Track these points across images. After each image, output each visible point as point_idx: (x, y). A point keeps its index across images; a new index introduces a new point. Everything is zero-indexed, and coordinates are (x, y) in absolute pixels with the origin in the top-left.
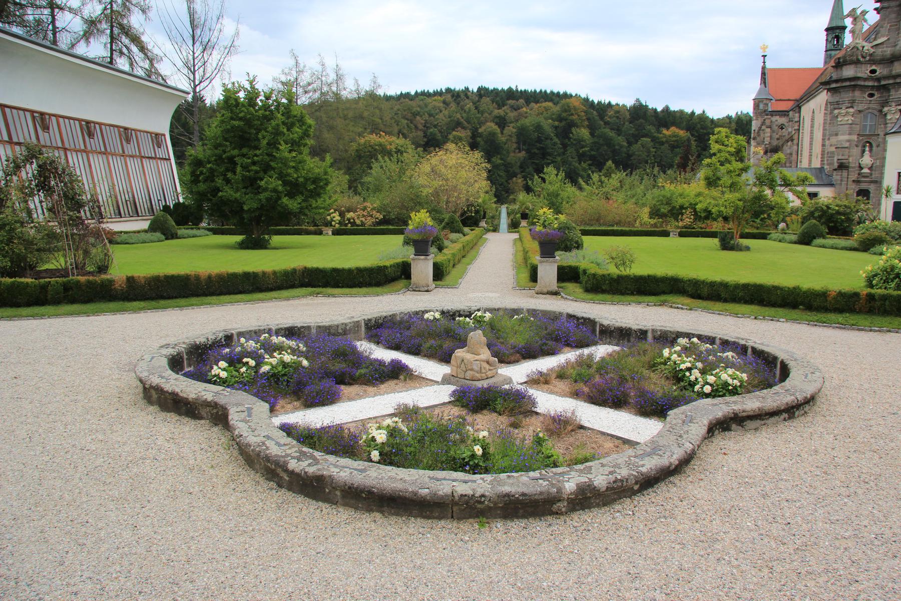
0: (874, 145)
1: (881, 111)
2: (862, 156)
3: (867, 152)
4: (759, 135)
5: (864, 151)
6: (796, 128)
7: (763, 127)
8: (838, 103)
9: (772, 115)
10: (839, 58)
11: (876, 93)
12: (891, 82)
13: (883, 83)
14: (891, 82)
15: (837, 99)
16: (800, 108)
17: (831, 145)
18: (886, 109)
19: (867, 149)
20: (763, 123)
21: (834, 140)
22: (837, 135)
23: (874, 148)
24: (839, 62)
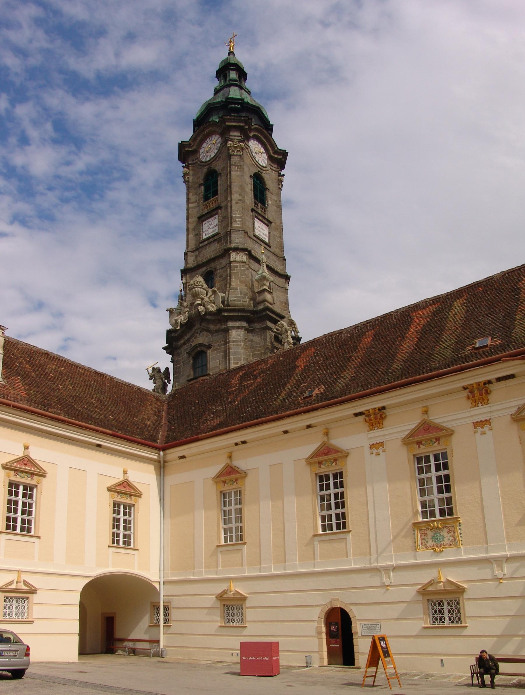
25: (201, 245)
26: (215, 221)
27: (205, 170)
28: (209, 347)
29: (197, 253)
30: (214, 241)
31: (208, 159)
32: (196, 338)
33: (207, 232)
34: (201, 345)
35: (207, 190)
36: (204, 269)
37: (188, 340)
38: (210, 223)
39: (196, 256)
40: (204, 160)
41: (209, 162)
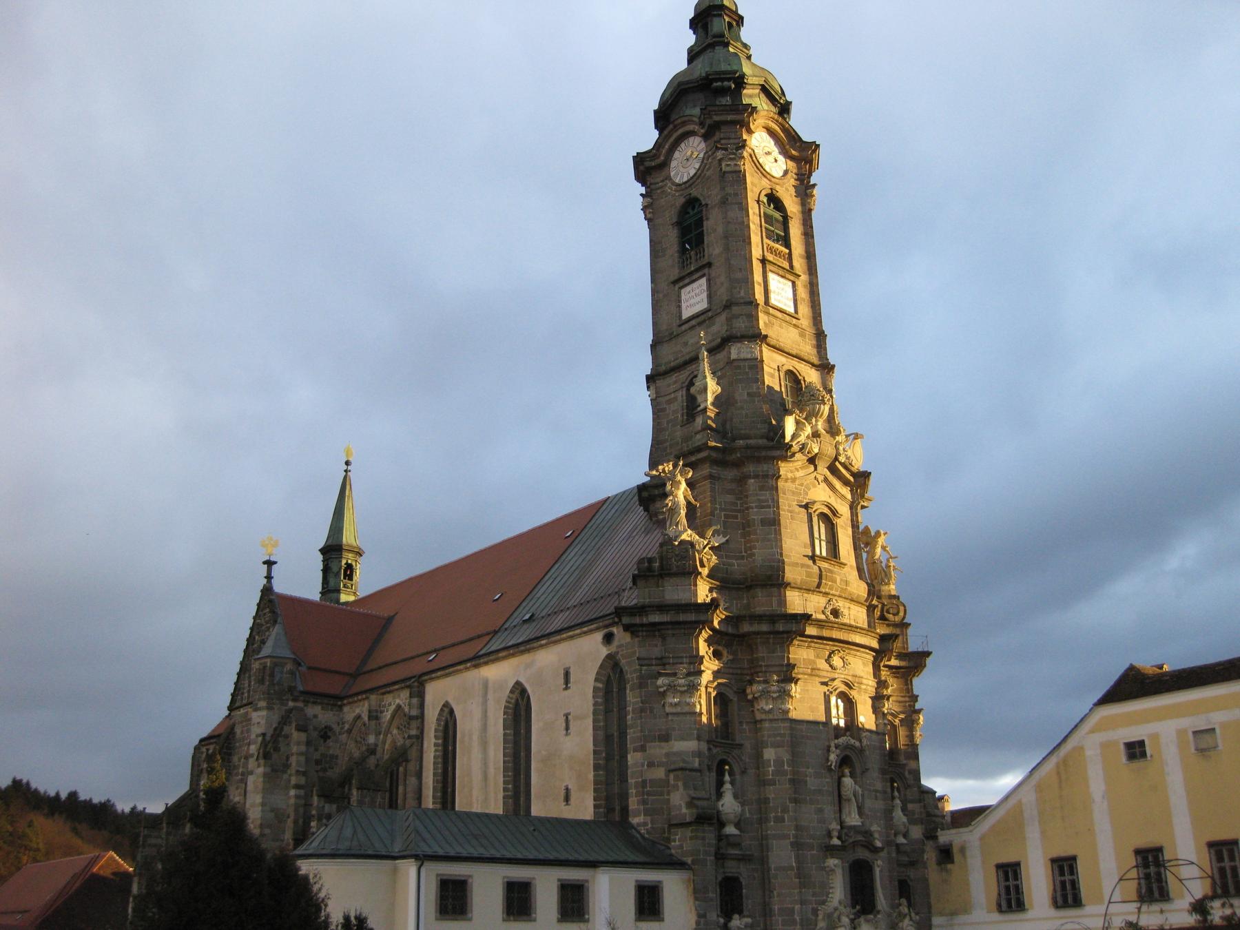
0: (736, 769)
1: (743, 692)
2: (719, 795)
3: (727, 786)
4: (277, 749)
5: (720, 783)
6: (414, 732)
7: (286, 729)
8: (662, 662)
9: (306, 702)
10: (650, 560)
11: (725, 653)
12: (765, 627)
13: (746, 628)
14: (765, 627)
15: (656, 651)
16: (422, 685)
17: (651, 765)
18: (756, 688)
19: (727, 778)
20: (285, 721)
21: (658, 750)
22: (665, 738)
23: (738, 777)
24: (650, 569)
25: (771, 311)
27: (765, 183)
32: (814, 486)
34: (829, 506)
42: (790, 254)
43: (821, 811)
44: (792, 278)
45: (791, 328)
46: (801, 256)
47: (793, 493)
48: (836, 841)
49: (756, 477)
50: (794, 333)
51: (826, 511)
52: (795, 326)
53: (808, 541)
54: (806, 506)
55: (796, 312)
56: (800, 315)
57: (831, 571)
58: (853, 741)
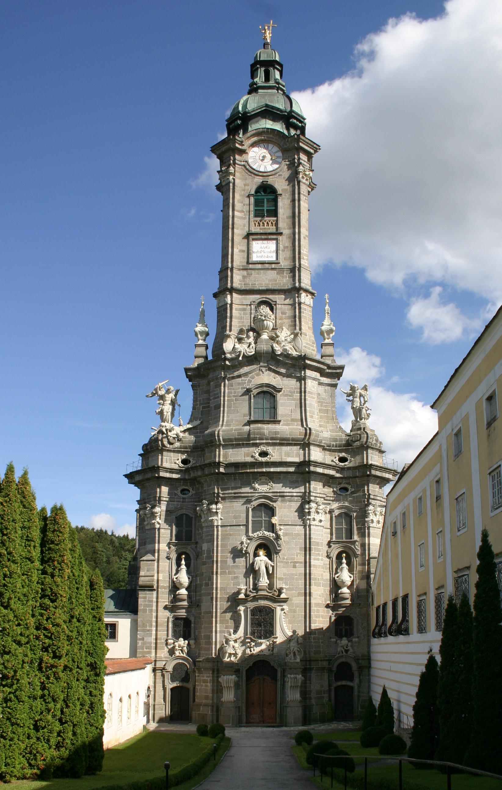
25: (251, 266)
26: (272, 245)
27: (259, 180)
28: (279, 390)
29: (245, 273)
30: (272, 269)
31: (262, 169)
32: (258, 375)
33: (259, 255)
34: (268, 385)
35: (258, 203)
36: (258, 296)
37: (246, 374)
38: (265, 245)
39: (244, 277)
40: (254, 167)
41: (265, 174)
42: (277, 221)
43: (237, 578)
44: (274, 237)
45: (270, 272)
46: (287, 218)
47: (239, 384)
48: (242, 596)
49: (213, 380)
50: (272, 274)
51: (265, 389)
52: (272, 269)
53: (247, 412)
54: (248, 392)
55: (277, 259)
56: (281, 260)
57: (260, 429)
58: (267, 533)
